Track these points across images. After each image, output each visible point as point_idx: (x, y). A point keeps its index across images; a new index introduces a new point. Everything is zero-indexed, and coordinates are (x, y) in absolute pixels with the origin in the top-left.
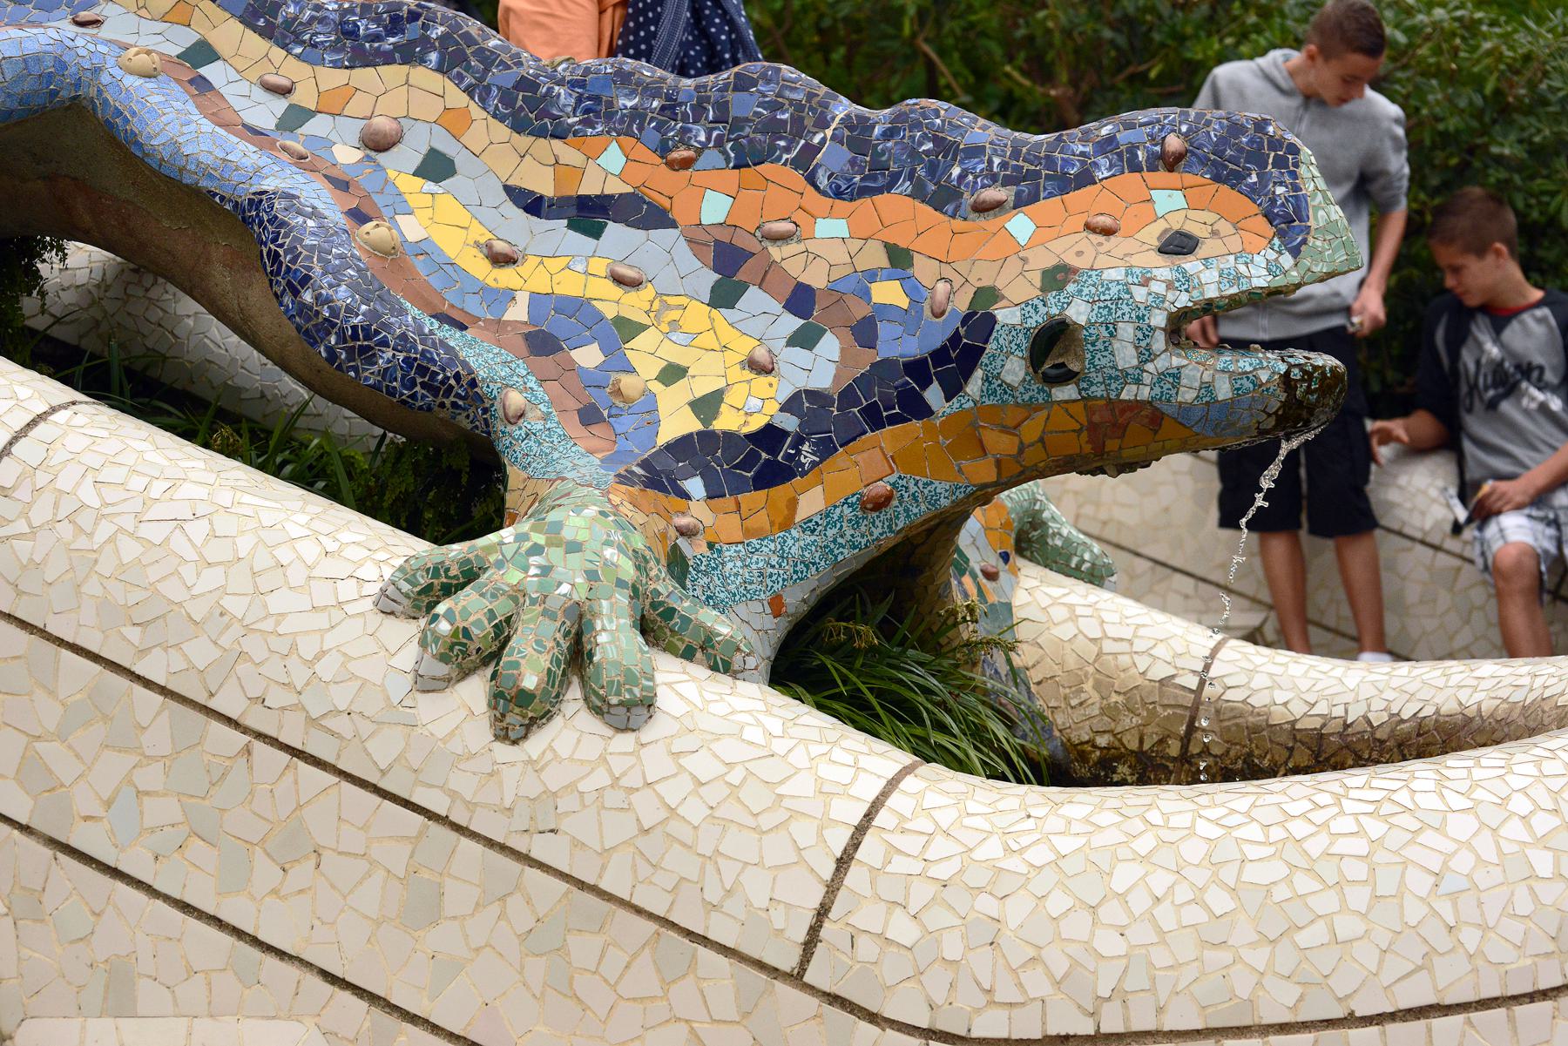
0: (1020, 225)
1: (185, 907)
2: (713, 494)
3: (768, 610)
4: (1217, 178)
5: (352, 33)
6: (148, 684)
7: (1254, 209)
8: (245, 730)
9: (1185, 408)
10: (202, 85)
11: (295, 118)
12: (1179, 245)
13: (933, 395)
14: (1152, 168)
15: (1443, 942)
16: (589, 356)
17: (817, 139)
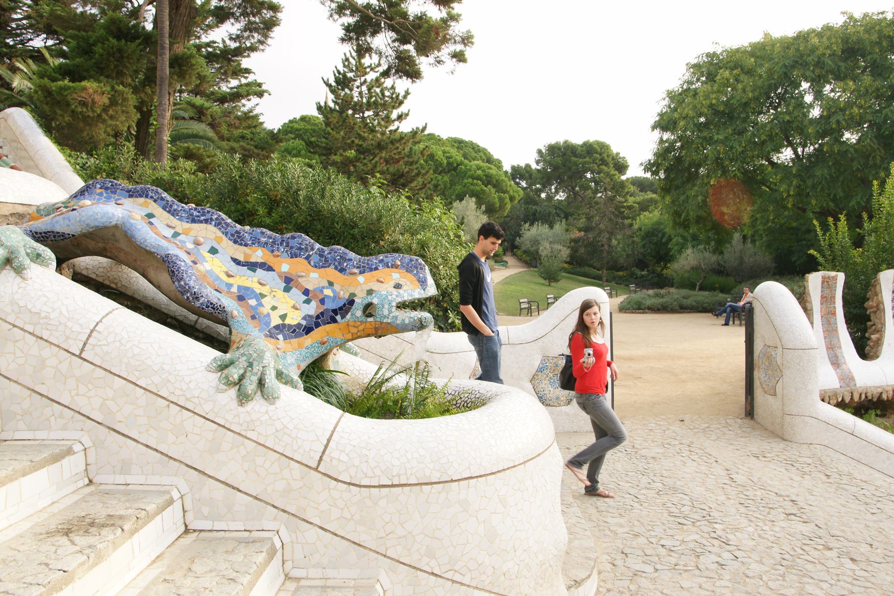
0: (361, 279)
1: (147, 446)
2: (285, 339)
4: (407, 271)
5: (192, 215)
6: (141, 387)
8: (168, 401)
10: (151, 223)
11: (176, 235)
12: (398, 286)
13: (338, 318)
14: (392, 267)
16: (253, 302)
17: (311, 253)
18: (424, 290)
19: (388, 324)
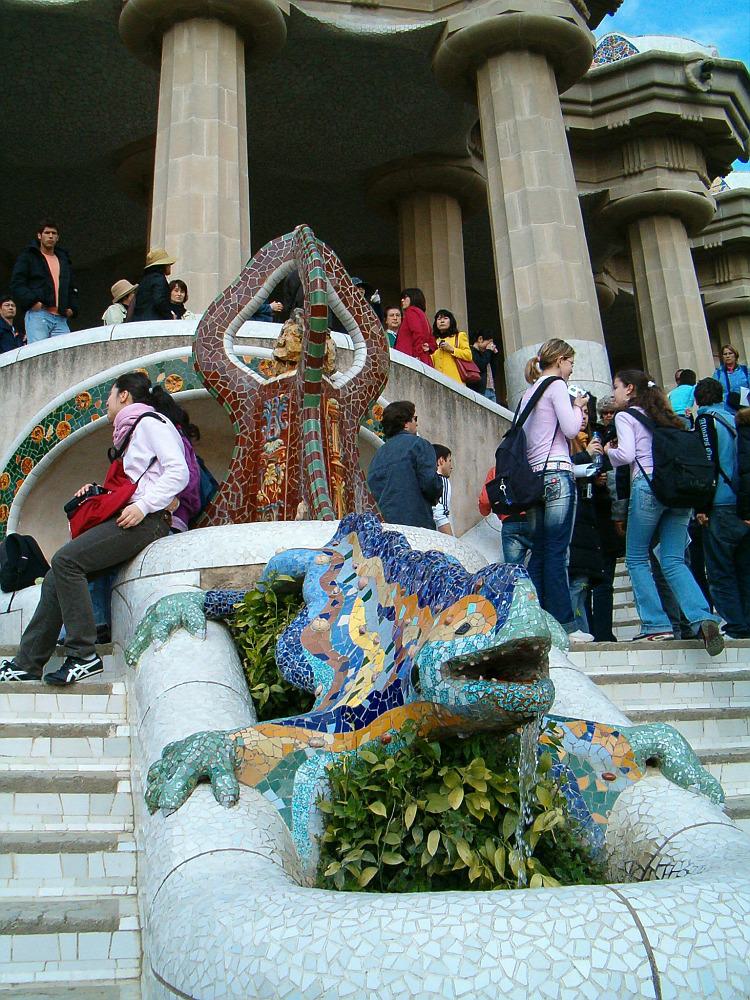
2: (337, 730)
4: (488, 598)
9: (453, 708)
12: (465, 629)
13: (404, 696)
15: (221, 975)
16: (351, 672)
18: (497, 631)
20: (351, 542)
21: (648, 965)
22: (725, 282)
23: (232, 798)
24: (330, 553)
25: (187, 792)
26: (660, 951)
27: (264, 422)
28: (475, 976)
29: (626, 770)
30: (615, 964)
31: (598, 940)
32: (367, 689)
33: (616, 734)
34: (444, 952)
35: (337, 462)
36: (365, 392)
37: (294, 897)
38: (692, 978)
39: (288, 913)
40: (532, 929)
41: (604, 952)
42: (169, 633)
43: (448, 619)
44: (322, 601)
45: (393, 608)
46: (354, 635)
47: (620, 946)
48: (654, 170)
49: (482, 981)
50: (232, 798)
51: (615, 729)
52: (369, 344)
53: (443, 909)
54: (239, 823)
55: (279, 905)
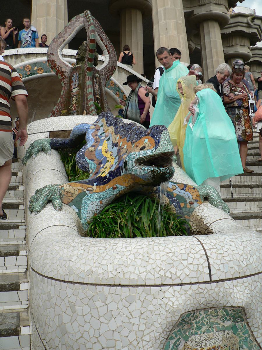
2: (97, 185)
3: (99, 202)
7: (154, 142)
13: (121, 172)
16: (102, 165)
18: (156, 149)
19: (134, 175)
20: (103, 121)
21: (207, 262)
22: (231, 46)
23: (60, 208)
24: (95, 125)
25: (44, 206)
26: (211, 257)
27: (72, 82)
28: (146, 266)
29: (197, 201)
30: (195, 262)
31: (190, 254)
32: (108, 171)
33: (194, 188)
34: (136, 258)
35: (98, 96)
36: (108, 72)
37: (82, 240)
38: (221, 267)
39: (80, 245)
40: (167, 250)
41: (192, 258)
42: (38, 153)
43: (138, 144)
44: (92, 141)
45: (117, 143)
46: (103, 153)
47: (198, 256)
48: (210, 4)
49: (149, 268)
50: (60, 208)
51: (194, 187)
52: (110, 56)
53: (135, 243)
54: (62, 216)
55: (77, 243)
